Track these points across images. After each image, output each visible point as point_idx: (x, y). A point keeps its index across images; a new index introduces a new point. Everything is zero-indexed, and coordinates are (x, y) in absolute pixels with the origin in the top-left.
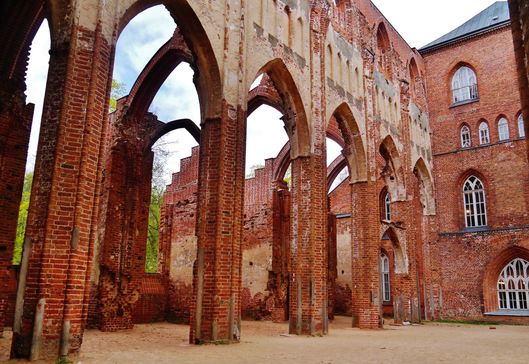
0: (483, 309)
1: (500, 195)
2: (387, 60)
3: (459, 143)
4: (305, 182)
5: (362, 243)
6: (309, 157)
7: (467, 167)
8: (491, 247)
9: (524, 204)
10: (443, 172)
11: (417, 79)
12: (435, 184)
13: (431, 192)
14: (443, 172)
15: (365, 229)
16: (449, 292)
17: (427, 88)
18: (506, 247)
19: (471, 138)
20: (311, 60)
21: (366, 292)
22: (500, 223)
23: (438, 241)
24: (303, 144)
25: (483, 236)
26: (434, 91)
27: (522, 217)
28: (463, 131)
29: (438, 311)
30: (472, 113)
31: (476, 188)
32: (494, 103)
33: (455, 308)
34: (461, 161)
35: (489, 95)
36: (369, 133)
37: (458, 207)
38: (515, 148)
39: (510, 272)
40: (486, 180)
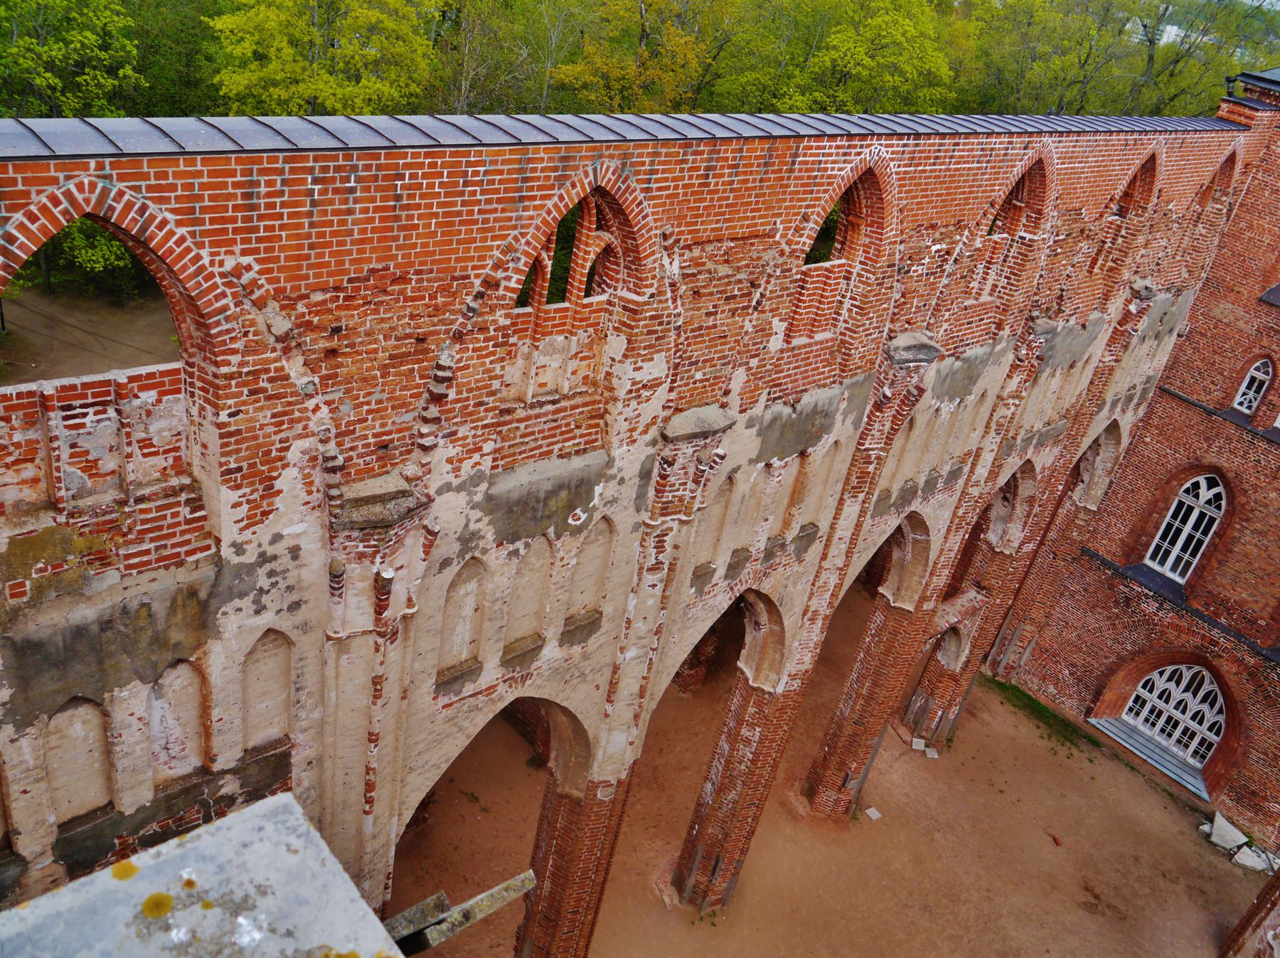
0: (1089, 712)
1: (1239, 557)
2: (1120, 240)
3: (1230, 397)
4: (752, 726)
5: (861, 702)
6: (770, 694)
7: (1215, 460)
8: (1163, 633)
9: (1273, 603)
10: (1159, 435)
11: (1218, 194)
12: (1128, 451)
13: (1109, 465)
14: (1159, 435)
15: (875, 684)
17: (1242, 205)
18: (1189, 650)
19: (1262, 402)
20: (835, 518)
21: (840, 770)
23: (1074, 559)
24: (766, 666)
25: (1161, 605)
26: (1251, 227)
27: (1253, 622)
28: (1257, 369)
29: (1012, 667)
31: (1209, 502)
33: (1044, 678)
34: (1207, 439)
36: (957, 520)
37: (1147, 522)
39: (1176, 677)
40: (1234, 509)
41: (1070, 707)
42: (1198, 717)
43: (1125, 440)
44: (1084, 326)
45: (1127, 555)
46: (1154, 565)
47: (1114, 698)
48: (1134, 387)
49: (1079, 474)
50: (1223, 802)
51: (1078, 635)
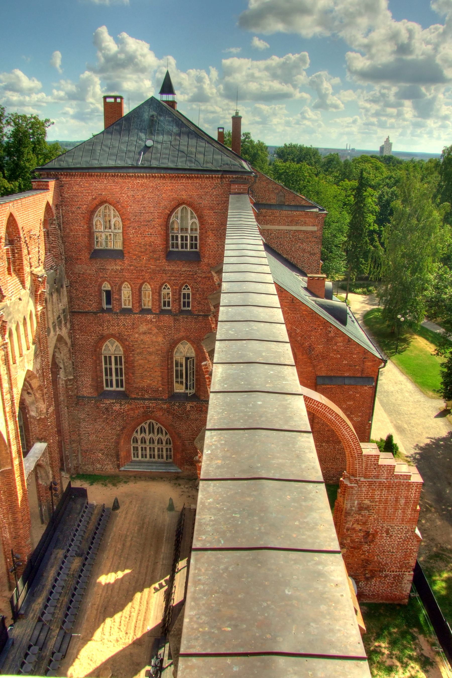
0: (119, 466)
2: (16, 255)
3: (100, 303)
9: (160, 379)
13: (68, 355)
14: (81, 333)
16: (87, 450)
17: (63, 223)
22: (137, 393)
25: (121, 403)
27: (157, 391)
29: (78, 467)
30: (115, 272)
32: (140, 267)
34: (100, 325)
35: (135, 255)
37: (96, 372)
38: (156, 322)
39: (143, 430)
41: (110, 468)
42: (160, 441)
43: (69, 341)
44: (20, 299)
45: (97, 390)
46: (109, 389)
47: (125, 454)
48: (59, 317)
49: (58, 366)
50: (187, 469)
51: (96, 436)
